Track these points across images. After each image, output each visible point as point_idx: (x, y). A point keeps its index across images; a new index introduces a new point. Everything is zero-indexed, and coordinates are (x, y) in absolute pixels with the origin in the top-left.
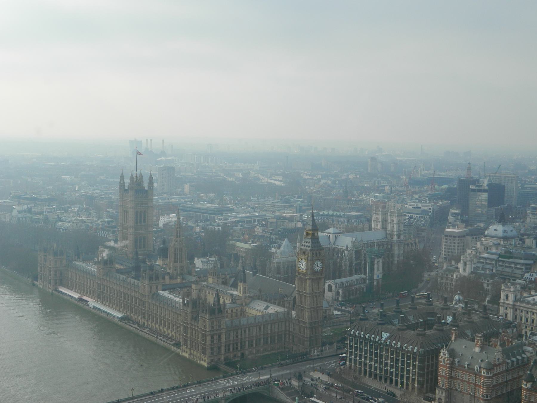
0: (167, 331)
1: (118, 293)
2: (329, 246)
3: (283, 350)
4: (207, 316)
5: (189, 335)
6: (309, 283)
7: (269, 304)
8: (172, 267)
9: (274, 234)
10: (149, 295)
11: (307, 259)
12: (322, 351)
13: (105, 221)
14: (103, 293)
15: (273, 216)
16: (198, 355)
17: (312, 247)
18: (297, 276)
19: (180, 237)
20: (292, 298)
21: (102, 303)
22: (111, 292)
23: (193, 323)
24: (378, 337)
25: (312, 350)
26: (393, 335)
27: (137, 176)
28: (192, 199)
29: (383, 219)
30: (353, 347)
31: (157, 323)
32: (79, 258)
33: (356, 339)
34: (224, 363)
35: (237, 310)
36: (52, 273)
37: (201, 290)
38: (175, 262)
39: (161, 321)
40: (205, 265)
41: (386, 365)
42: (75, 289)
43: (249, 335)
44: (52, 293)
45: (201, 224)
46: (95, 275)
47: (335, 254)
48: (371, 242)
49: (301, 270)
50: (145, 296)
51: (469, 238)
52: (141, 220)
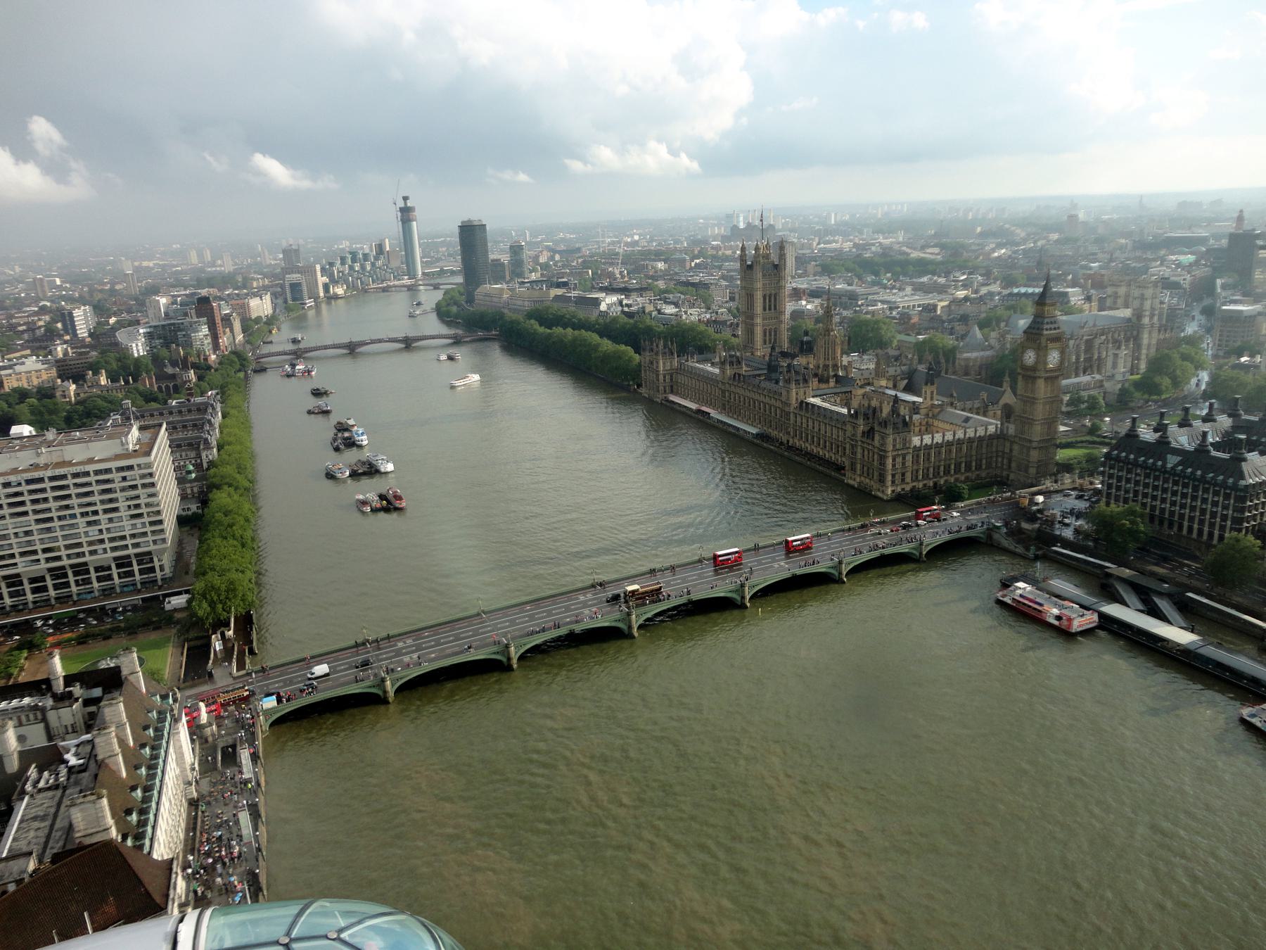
4: (890, 430)
7: (971, 415)
8: (821, 366)
16: (872, 482)
18: (1019, 374)
20: (1000, 407)
21: (728, 416)
23: (864, 440)
24: (1160, 463)
32: (693, 358)
35: (920, 424)
39: (813, 437)
41: (1173, 503)
44: (661, 403)
50: (789, 405)
51: (1260, 318)
52: (770, 306)
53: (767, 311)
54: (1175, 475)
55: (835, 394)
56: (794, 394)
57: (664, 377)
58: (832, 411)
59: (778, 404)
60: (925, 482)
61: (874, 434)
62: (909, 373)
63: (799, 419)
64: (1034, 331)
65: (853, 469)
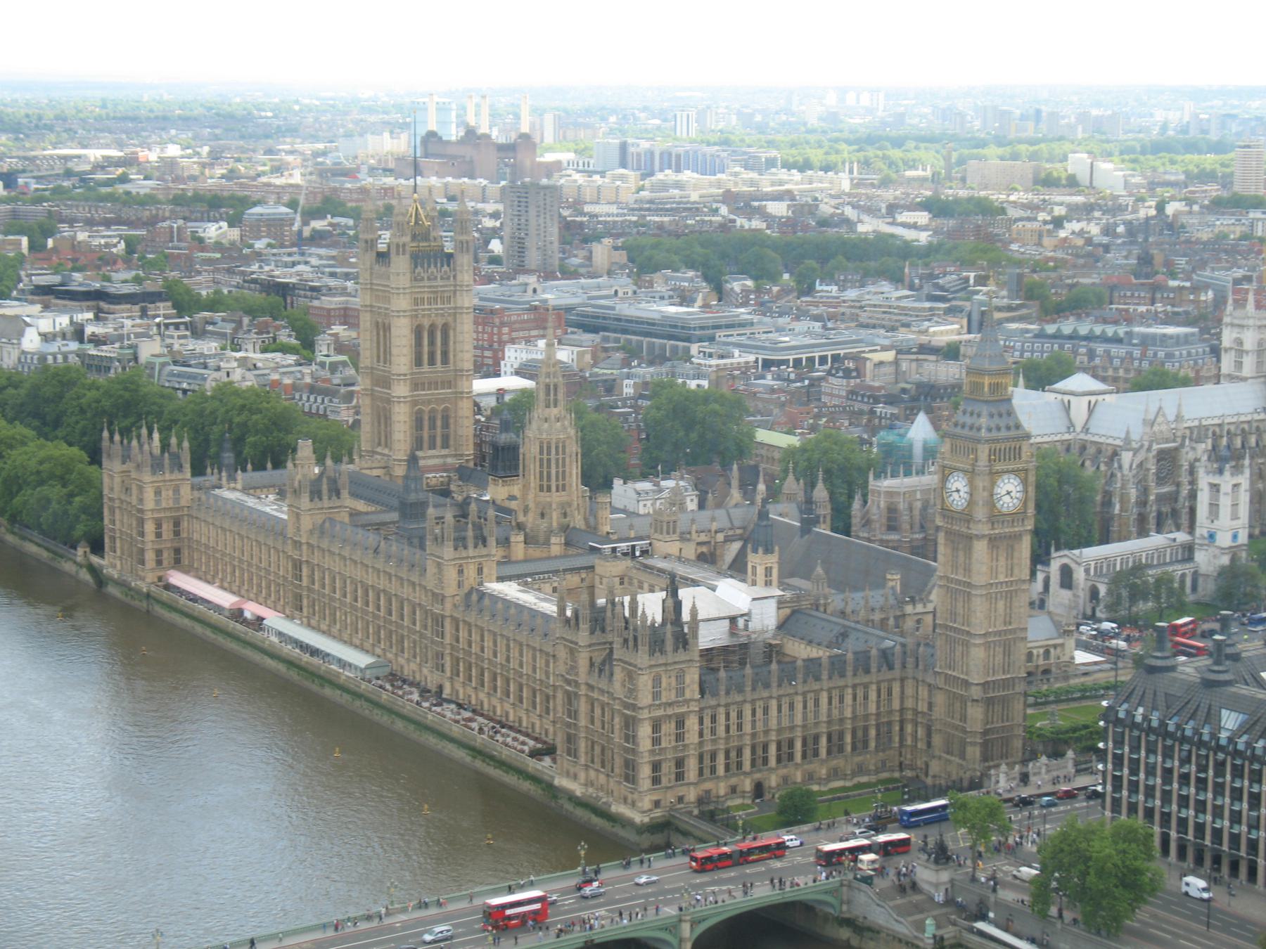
1: (356, 591)
2: (1067, 437)
3: (897, 775)
4: (642, 658)
6: (980, 548)
9: (885, 403)
12: (1025, 779)
13: (322, 365)
14: (309, 589)
15: (887, 342)
16: (612, 785)
17: (990, 430)
18: (938, 528)
19: (555, 406)
21: (309, 626)
22: (334, 589)
23: (591, 682)
24: (1206, 731)
25: (992, 772)
26: (1255, 723)
28: (616, 292)
29: (1260, 344)
30: (1126, 762)
31: (483, 686)
32: (232, 478)
33: (1136, 733)
34: (696, 812)
37: (626, 580)
38: (541, 489)
40: (649, 503)
41: (1236, 818)
42: (222, 580)
43: (779, 723)
45: (640, 371)
46: (282, 534)
47: (1088, 463)
48: (1216, 421)
49: (954, 508)
50: (442, 599)
53: (426, 368)
54: (1237, 753)
55: (556, 572)
56: (451, 574)
58: (534, 613)
59: (418, 597)
60: (734, 781)
61: (611, 666)
62: (744, 528)
63: (463, 634)
64: (966, 432)
65: (572, 752)
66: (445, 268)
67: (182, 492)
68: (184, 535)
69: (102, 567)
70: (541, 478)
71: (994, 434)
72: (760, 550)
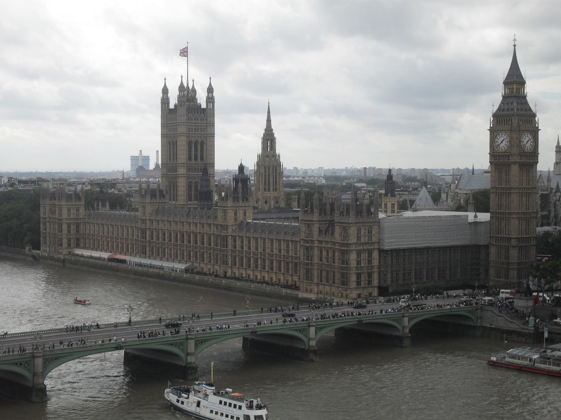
0: (268, 275)
1: (177, 236)
4: (352, 219)
5: (316, 260)
6: (515, 169)
10: (232, 225)
11: (511, 129)
17: (518, 110)
23: (320, 239)
27: (188, 87)
31: (249, 267)
32: (104, 205)
36: (63, 227)
38: (265, 190)
39: (256, 261)
44: (64, 261)
53: (193, 162)
56: (231, 214)
57: (69, 227)
59: (213, 230)
63: (238, 243)
64: (506, 113)
66: (202, 115)
67: (80, 210)
68: (81, 232)
69: (38, 254)
70: (265, 185)
71: (520, 112)
72: (389, 195)
